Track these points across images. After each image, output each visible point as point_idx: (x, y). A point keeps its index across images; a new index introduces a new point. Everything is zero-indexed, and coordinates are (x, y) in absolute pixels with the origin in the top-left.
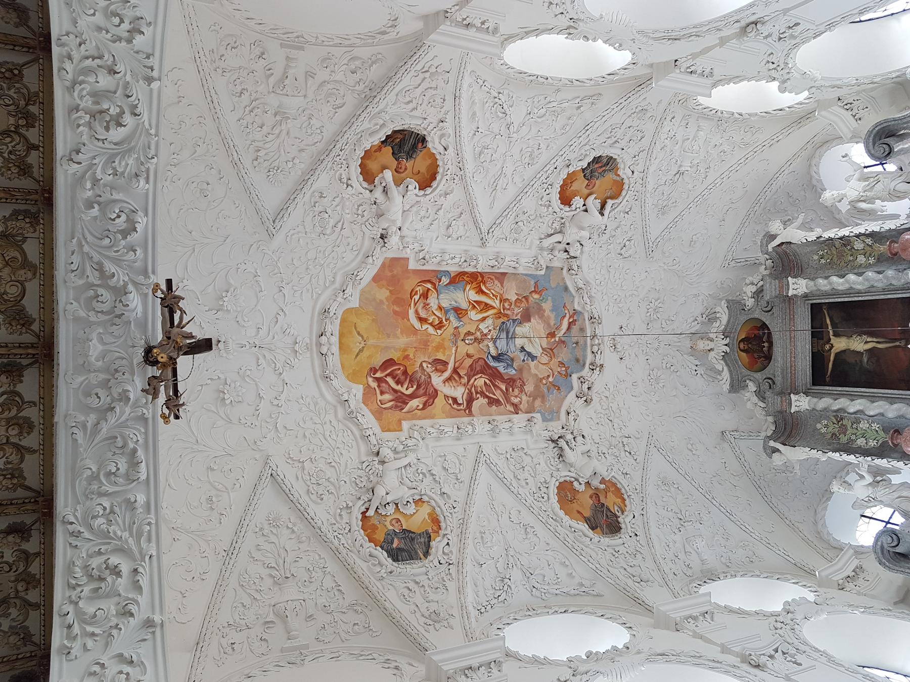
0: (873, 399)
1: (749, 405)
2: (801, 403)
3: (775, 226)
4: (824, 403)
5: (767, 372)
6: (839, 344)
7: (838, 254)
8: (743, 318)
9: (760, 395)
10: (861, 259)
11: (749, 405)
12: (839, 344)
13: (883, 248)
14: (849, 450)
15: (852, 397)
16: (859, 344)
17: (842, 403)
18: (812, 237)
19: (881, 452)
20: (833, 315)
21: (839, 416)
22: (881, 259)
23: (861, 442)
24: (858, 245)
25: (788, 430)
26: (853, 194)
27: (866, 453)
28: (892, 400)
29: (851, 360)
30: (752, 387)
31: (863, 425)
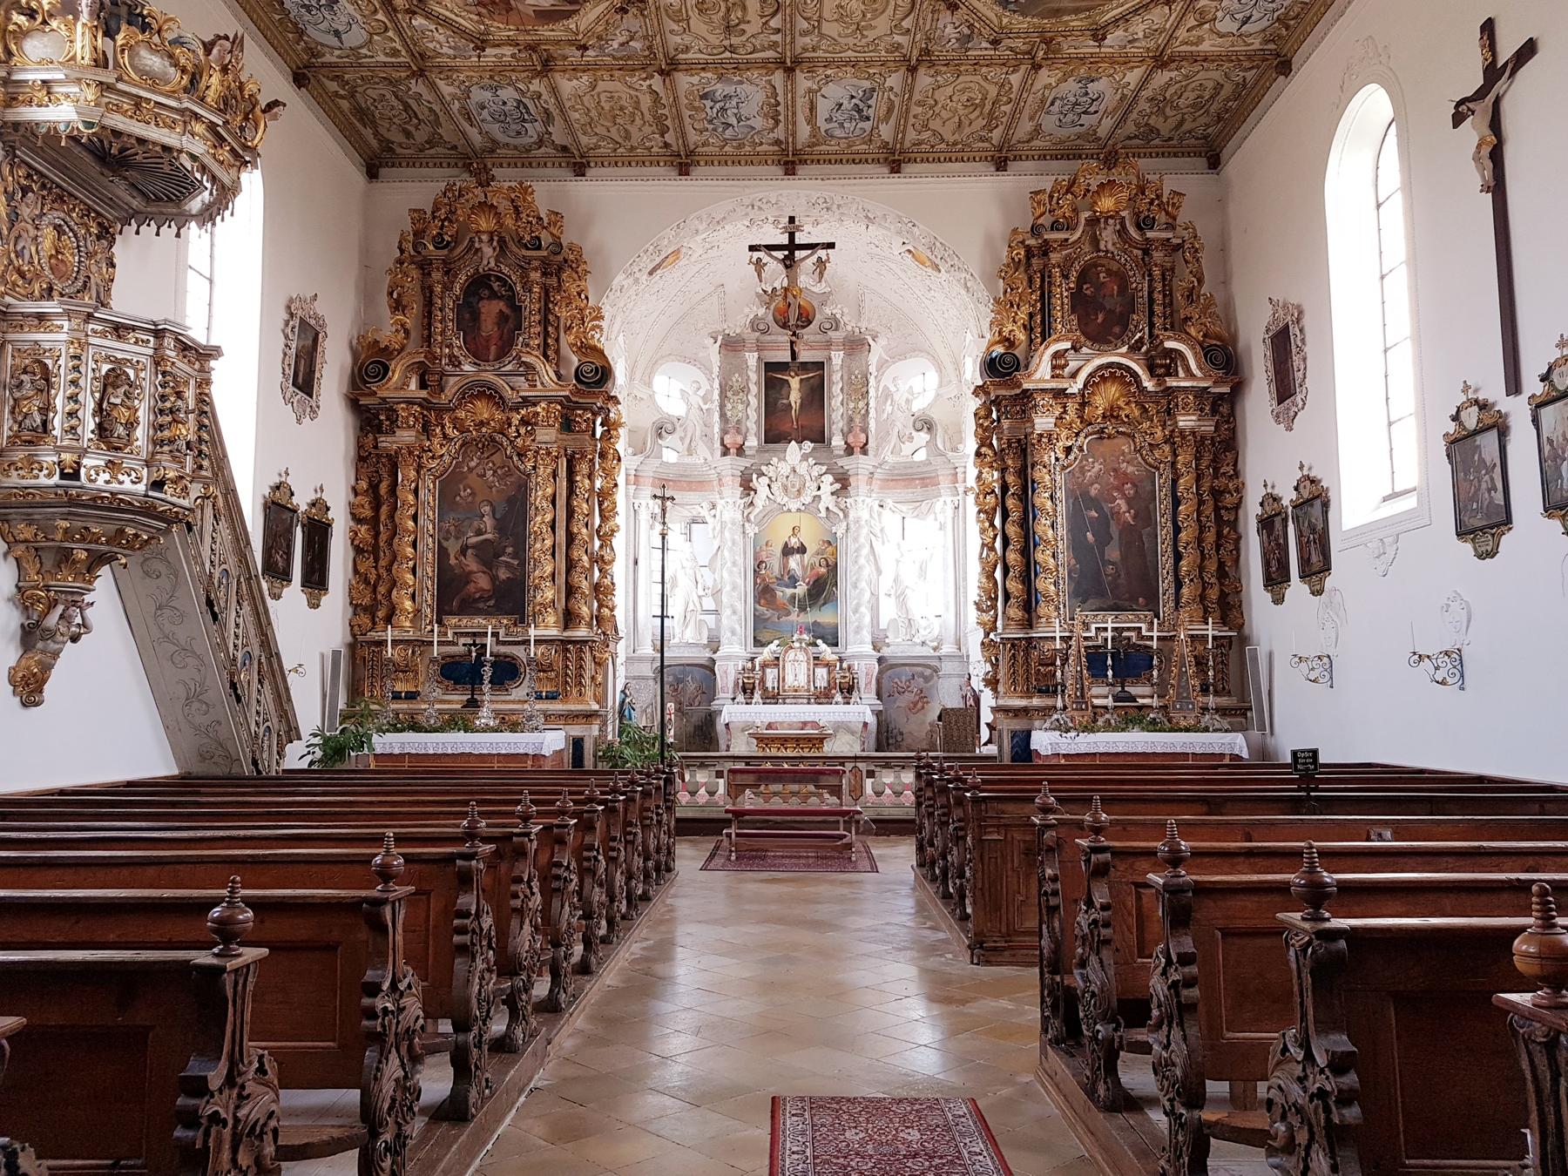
0: (758, 410)
1: (747, 310)
2: (752, 359)
3: (882, 341)
4: (753, 377)
5: (775, 328)
6: (795, 383)
7: (859, 388)
8: (815, 304)
9: (755, 325)
10: (852, 405)
11: (747, 310)
12: (795, 383)
13: (857, 420)
14: (723, 396)
15: (757, 396)
16: (795, 397)
17: (754, 389)
18: (872, 369)
19: (723, 415)
20: (815, 376)
21: (745, 390)
22: (851, 420)
23: (729, 406)
24: (861, 404)
25: (731, 345)
26: (896, 397)
27: (722, 406)
28: (758, 422)
29: (784, 392)
30: (761, 311)
31: (740, 407)
